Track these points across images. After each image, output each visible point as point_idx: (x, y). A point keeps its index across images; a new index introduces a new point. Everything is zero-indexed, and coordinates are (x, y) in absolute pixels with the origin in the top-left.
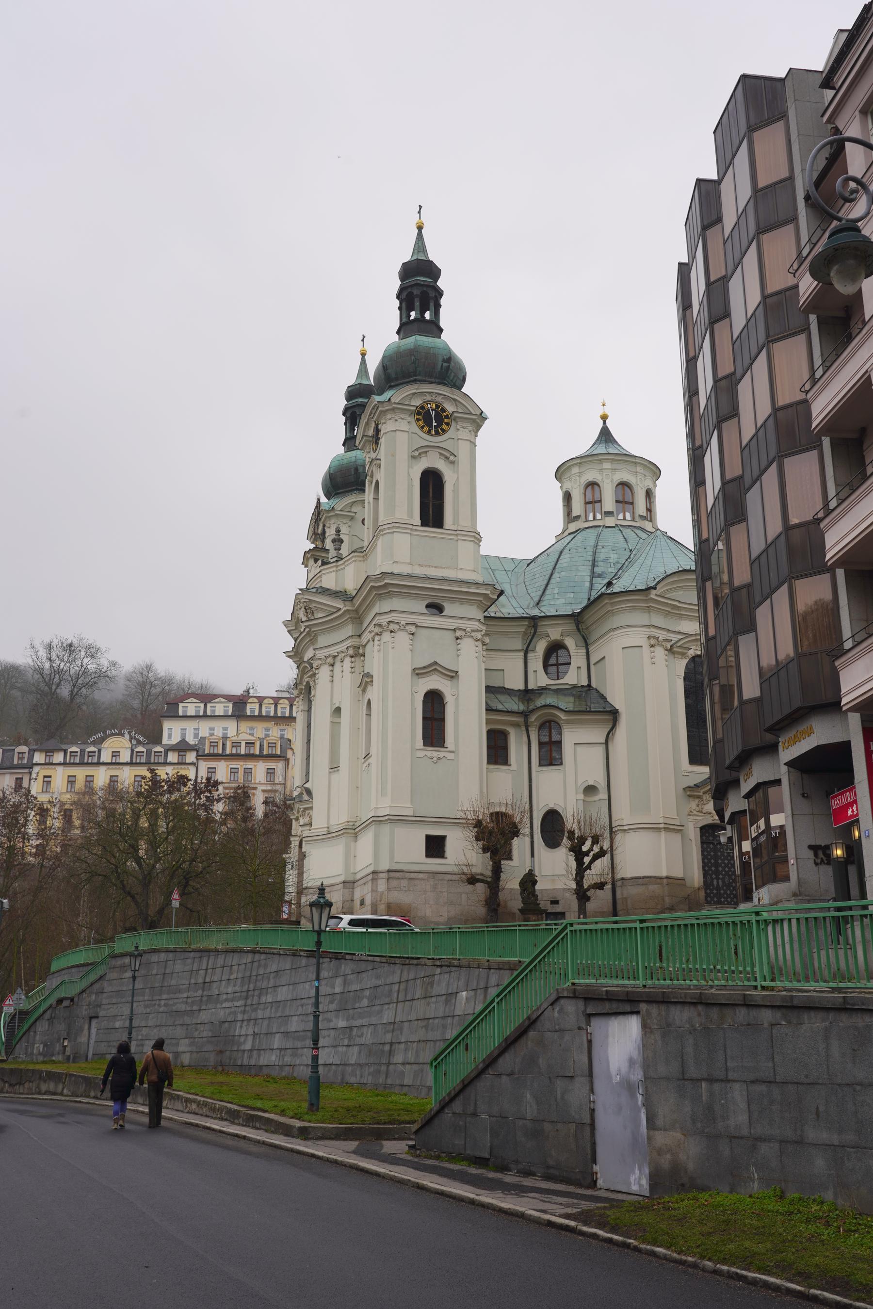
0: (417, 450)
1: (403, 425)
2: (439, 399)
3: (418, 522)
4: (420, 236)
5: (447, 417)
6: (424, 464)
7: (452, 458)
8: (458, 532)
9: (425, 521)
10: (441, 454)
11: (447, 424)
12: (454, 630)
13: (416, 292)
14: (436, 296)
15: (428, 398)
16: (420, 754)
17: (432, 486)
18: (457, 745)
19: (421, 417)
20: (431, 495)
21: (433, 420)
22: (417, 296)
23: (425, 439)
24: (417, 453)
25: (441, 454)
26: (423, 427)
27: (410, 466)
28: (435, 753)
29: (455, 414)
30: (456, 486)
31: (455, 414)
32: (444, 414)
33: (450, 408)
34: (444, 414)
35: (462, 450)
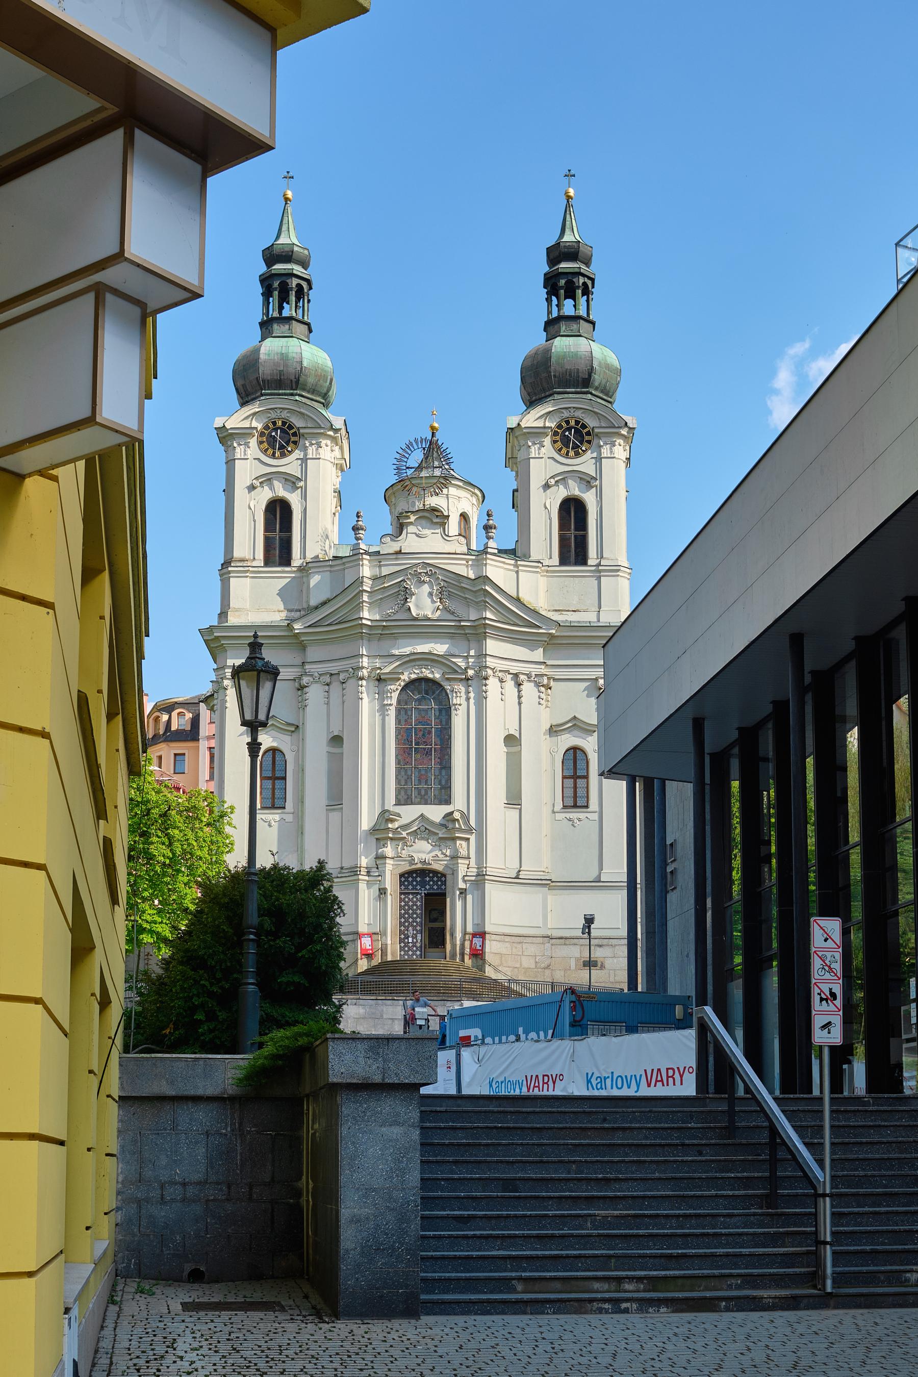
0: (552, 477)
2: (578, 414)
5: (588, 434)
6: (561, 493)
7: (592, 481)
8: (600, 568)
9: (564, 561)
10: (581, 479)
13: (562, 282)
14: (585, 284)
15: (566, 414)
16: (560, 816)
19: (558, 438)
20: (573, 527)
22: (562, 288)
24: (553, 481)
25: (581, 479)
26: (560, 450)
31: (596, 430)
32: (585, 431)
34: (585, 431)
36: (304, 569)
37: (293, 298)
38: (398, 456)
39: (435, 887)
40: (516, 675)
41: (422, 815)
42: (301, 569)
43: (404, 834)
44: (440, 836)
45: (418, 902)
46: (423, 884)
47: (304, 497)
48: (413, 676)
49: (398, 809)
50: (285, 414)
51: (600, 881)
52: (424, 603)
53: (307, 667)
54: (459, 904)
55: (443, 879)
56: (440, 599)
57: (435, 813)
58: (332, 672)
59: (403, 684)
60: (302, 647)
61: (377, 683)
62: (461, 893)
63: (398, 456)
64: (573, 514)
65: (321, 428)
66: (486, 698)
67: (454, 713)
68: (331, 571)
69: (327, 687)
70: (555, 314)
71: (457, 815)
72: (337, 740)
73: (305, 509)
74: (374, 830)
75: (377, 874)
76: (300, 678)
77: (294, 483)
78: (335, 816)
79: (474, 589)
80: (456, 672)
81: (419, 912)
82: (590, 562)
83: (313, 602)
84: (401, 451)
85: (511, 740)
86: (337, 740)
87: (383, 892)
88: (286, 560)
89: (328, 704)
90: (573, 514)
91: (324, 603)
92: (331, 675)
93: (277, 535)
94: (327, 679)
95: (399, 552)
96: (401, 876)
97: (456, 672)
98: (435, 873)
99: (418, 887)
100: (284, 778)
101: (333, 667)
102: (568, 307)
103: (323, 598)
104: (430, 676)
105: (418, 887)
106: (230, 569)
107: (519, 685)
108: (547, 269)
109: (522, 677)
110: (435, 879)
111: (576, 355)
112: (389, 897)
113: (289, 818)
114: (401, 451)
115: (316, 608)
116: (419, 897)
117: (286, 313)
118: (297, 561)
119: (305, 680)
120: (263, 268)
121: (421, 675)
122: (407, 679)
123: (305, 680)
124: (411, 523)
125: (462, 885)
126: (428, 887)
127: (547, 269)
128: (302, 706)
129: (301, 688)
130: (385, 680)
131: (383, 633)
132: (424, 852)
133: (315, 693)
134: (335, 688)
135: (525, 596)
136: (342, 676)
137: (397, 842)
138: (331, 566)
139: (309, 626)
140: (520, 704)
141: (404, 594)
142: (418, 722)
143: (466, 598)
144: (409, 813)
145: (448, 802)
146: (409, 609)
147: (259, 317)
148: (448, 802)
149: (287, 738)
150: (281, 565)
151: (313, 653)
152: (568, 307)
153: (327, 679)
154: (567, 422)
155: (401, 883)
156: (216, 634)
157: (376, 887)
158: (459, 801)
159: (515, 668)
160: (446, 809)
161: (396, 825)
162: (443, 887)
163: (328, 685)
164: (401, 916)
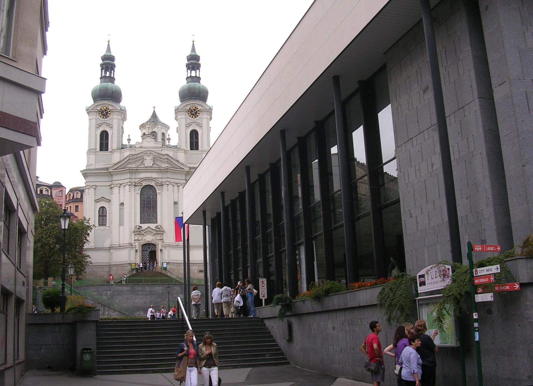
1: (183, 116)
2: (196, 105)
3: (189, 149)
4: (193, 44)
6: (191, 128)
9: (192, 149)
15: (192, 105)
21: (194, 113)
23: (190, 119)
27: (186, 130)
33: (200, 108)
35: (205, 122)
37: (109, 70)
42: (111, 152)
45: (147, 253)
46: (149, 248)
47: (112, 130)
49: (141, 225)
50: (107, 105)
52: (148, 162)
57: (153, 226)
60: (112, 175)
64: (194, 135)
67: (158, 195)
70: (189, 76)
71: (159, 227)
72: (122, 204)
74: (134, 232)
78: (121, 228)
83: (115, 162)
87: (136, 251)
88: (107, 150)
90: (194, 135)
91: (118, 163)
93: (104, 141)
94: (119, 185)
96: (142, 245)
98: (153, 244)
100: (106, 216)
102: (193, 74)
103: (118, 160)
108: (187, 62)
109: (178, 185)
111: (195, 88)
113: (108, 228)
117: (108, 74)
118: (110, 149)
119: (112, 186)
120: (101, 62)
125: (160, 248)
127: (187, 62)
129: (111, 188)
131: (136, 171)
132: (149, 238)
133: (116, 190)
134: (122, 187)
135: (179, 159)
136: (124, 185)
142: (147, 198)
144: (145, 226)
145: (157, 223)
147: (100, 76)
148: (157, 223)
149: (107, 204)
150: (105, 151)
151: (115, 178)
152: (193, 74)
153: (119, 185)
155: (142, 248)
157: (134, 249)
158: (159, 223)
159: (177, 181)
160: (156, 225)
164: (142, 258)
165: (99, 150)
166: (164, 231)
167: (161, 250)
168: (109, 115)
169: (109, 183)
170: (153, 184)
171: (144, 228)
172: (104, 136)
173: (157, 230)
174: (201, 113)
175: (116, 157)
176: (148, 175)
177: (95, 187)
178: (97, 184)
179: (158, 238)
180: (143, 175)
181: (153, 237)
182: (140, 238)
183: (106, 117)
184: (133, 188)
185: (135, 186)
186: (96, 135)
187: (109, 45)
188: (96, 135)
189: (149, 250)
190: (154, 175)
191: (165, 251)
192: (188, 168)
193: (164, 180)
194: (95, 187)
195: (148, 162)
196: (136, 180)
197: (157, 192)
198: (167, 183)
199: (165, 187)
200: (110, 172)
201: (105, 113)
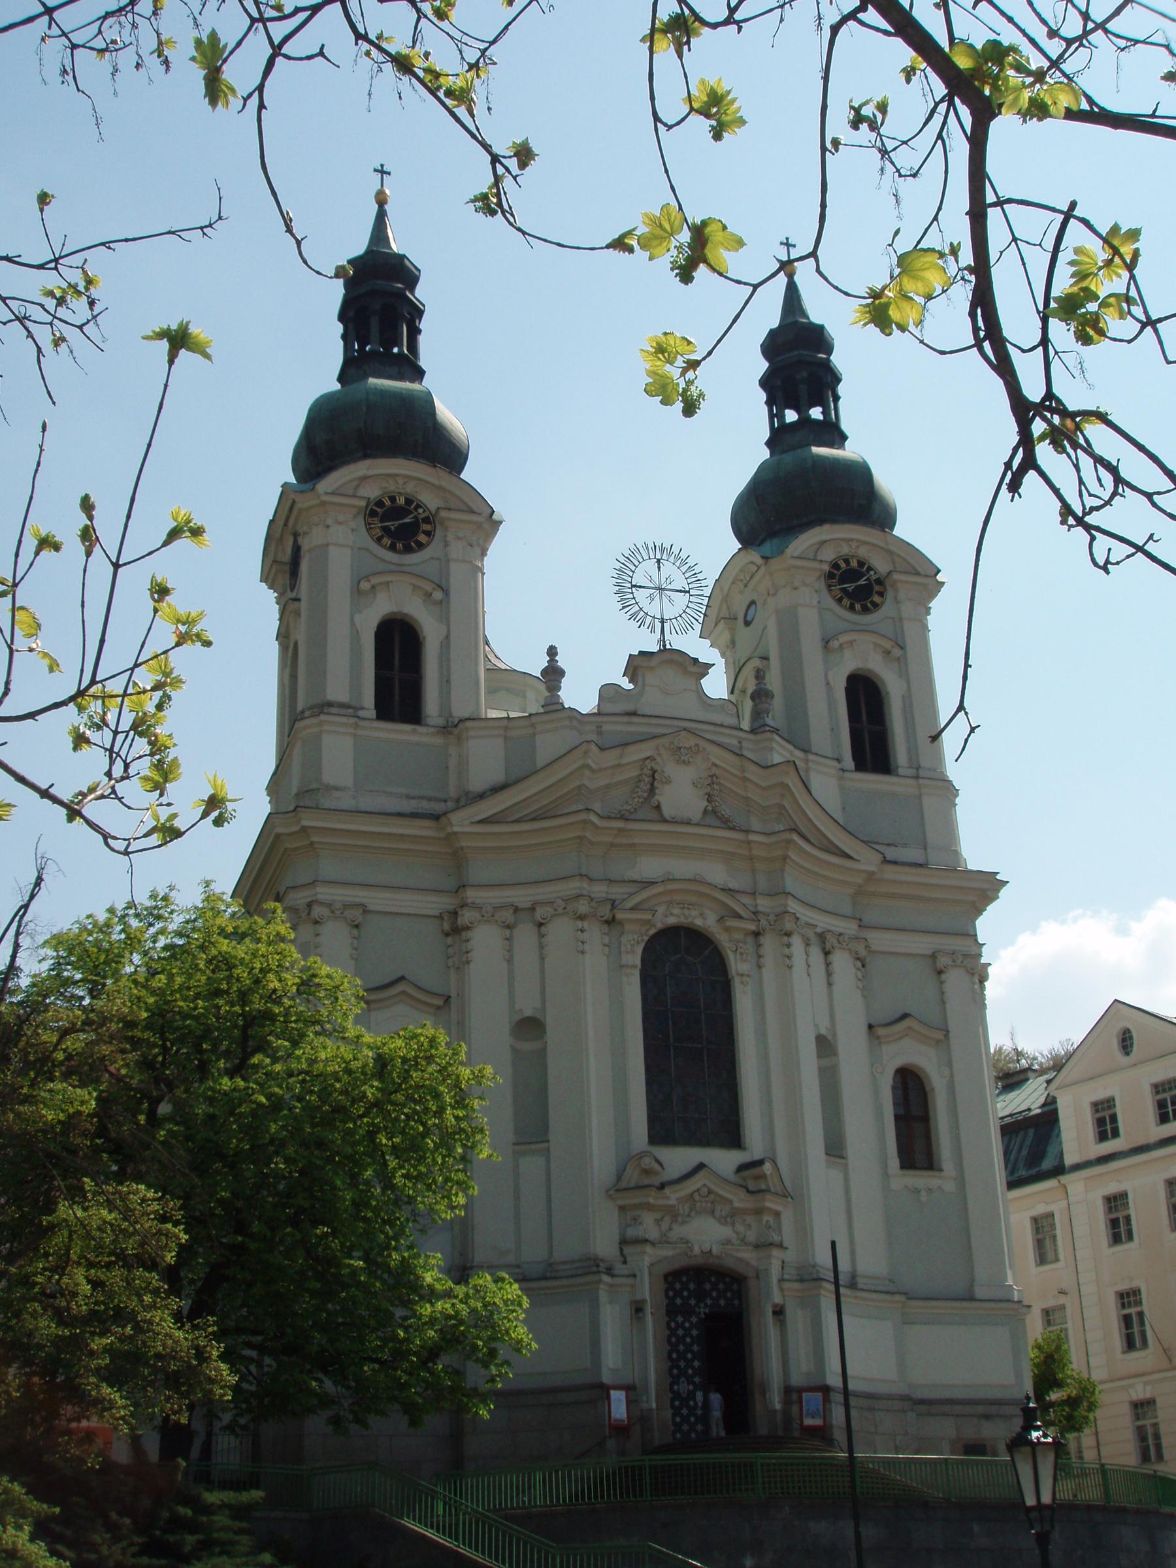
6: (849, 664)
10: (876, 645)
11: (881, 594)
12: (933, 956)
15: (845, 550)
17: (865, 699)
18: (959, 1165)
20: (864, 717)
25: (876, 645)
28: (920, 1180)
29: (896, 576)
30: (908, 701)
36: (450, 733)
38: (618, 566)
39: (722, 1302)
40: (822, 937)
41: (701, 1166)
43: (672, 1202)
44: (737, 1204)
47: (445, 619)
48: (672, 921)
50: (410, 488)
51: (972, 1299)
53: (471, 894)
54: (772, 1332)
55: (735, 1287)
56: (709, 795)
57: (724, 1160)
58: (521, 905)
59: (652, 932)
61: (605, 926)
62: (775, 1313)
63: (618, 566)
65: (472, 512)
66: (790, 967)
68: (505, 738)
69: (508, 932)
72: (530, 1027)
73: (447, 637)
75: (626, 1272)
76: (455, 914)
77: (429, 595)
78: (531, 1165)
79: (764, 784)
80: (739, 917)
81: (695, 1348)
82: (901, 771)
83: (477, 784)
84: (622, 559)
85: (825, 1045)
86: (530, 1027)
87: (638, 1309)
89: (510, 961)
90: (865, 699)
92: (516, 910)
95: (634, 714)
96: (666, 1277)
97: (739, 917)
99: (693, 1302)
101: (521, 897)
104: (699, 922)
105: (709, 1302)
106: (323, 717)
107: (827, 954)
110: (721, 1286)
112: (649, 1319)
114: (622, 559)
115: (481, 796)
116: (694, 1320)
121: (683, 920)
122: (659, 926)
123: (466, 916)
124: (652, 668)
125: (777, 1299)
126: (709, 1302)
128: (460, 963)
130: (621, 923)
132: (707, 1235)
133: (485, 941)
134: (525, 935)
136: (540, 913)
137: (658, 1215)
138: (506, 728)
139: (481, 822)
140: (830, 984)
141: (652, 780)
143: (747, 799)
144: (677, 1159)
146: (658, 807)
154: (847, 561)
156: (305, 823)
161: (656, 1181)
162: (736, 1302)
163: (508, 927)
165: (372, 713)
166: (785, 1195)
167: (779, 1312)
168: (422, 538)
169: (444, 903)
170: (706, 920)
171: (672, 1173)
172: (398, 646)
173: (752, 1186)
174: (890, 594)
175: (484, 762)
176: (682, 867)
177: (357, 914)
178: (377, 900)
179: (751, 1236)
180: (650, 867)
181: (725, 1232)
182: (653, 1234)
183: (408, 550)
184: (595, 934)
185: (611, 922)
186: (355, 635)
187: (381, 216)
188: (355, 635)
189: (703, 1310)
190: (717, 873)
191: (797, 1318)
192: (877, 858)
193: (763, 904)
194: (357, 914)
195: (681, 793)
196: (617, 891)
197: (737, 965)
198: (789, 925)
199: (769, 943)
200: (450, 838)
201: (401, 526)
